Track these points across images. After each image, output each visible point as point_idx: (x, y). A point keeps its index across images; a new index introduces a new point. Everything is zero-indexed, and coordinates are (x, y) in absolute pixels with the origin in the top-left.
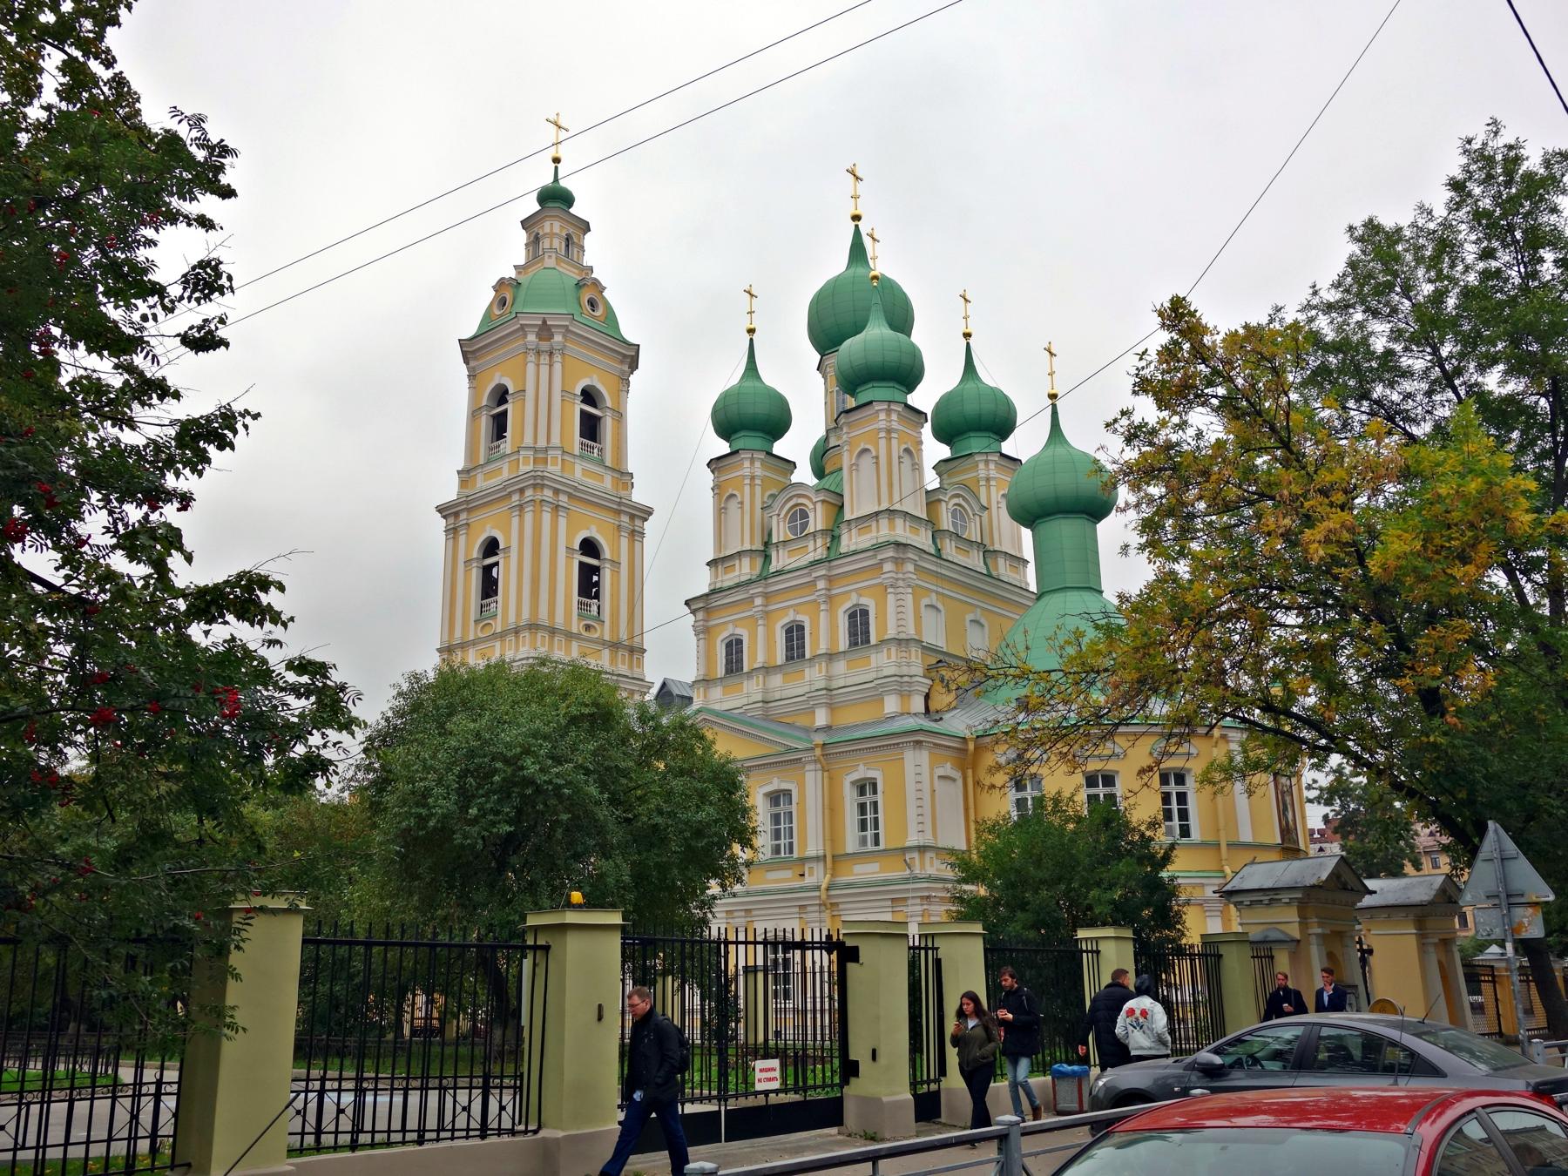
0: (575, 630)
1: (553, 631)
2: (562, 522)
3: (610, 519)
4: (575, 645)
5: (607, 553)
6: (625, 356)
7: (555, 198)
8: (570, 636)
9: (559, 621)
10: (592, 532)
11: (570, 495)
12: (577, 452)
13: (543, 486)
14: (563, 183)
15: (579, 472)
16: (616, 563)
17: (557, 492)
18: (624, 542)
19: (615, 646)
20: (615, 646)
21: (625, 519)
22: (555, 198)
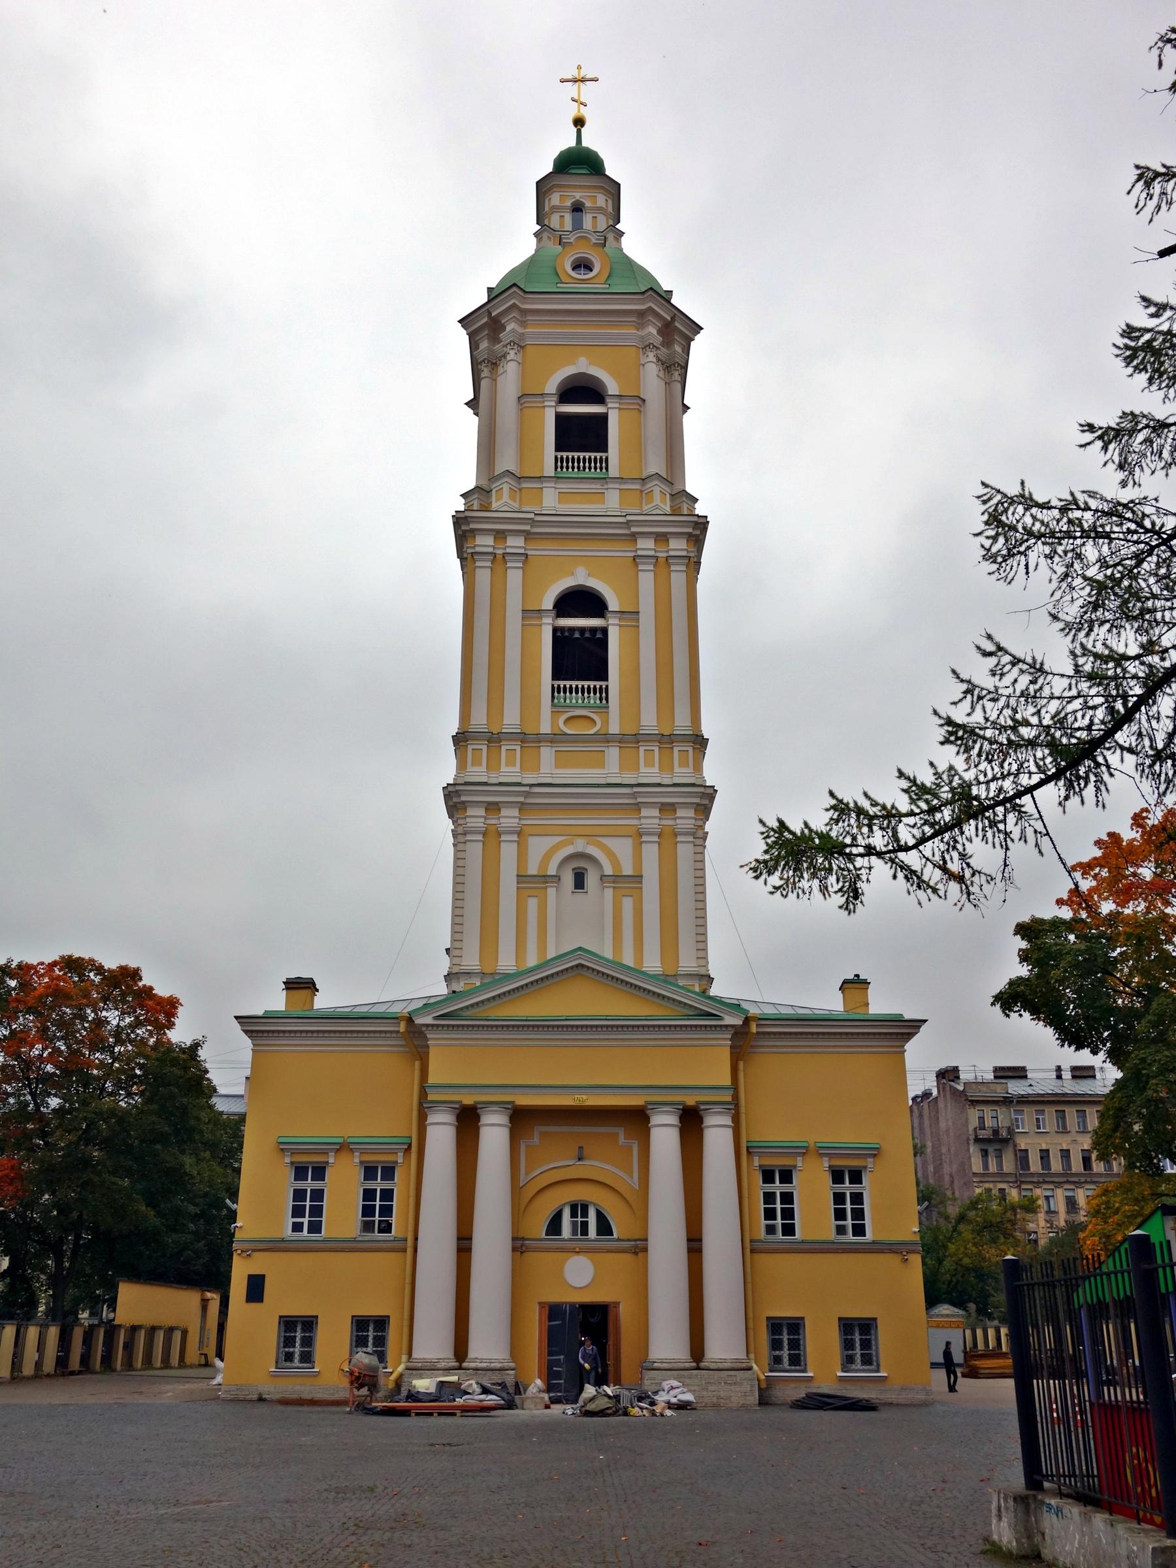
0: (546, 728)
1: (494, 739)
2: (514, 577)
3: (622, 552)
4: (547, 754)
5: (613, 604)
6: (641, 314)
7: (579, 164)
8: (528, 740)
9: (511, 719)
10: (581, 577)
11: (528, 536)
12: (549, 470)
13: (473, 531)
14: (585, 144)
15: (550, 500)
16: (631, 616)
17: (500, 535)
18: (647, 579)
19: (631, 740)
20: (631, 740)
21: (646, 545)
22: (579, 164)
